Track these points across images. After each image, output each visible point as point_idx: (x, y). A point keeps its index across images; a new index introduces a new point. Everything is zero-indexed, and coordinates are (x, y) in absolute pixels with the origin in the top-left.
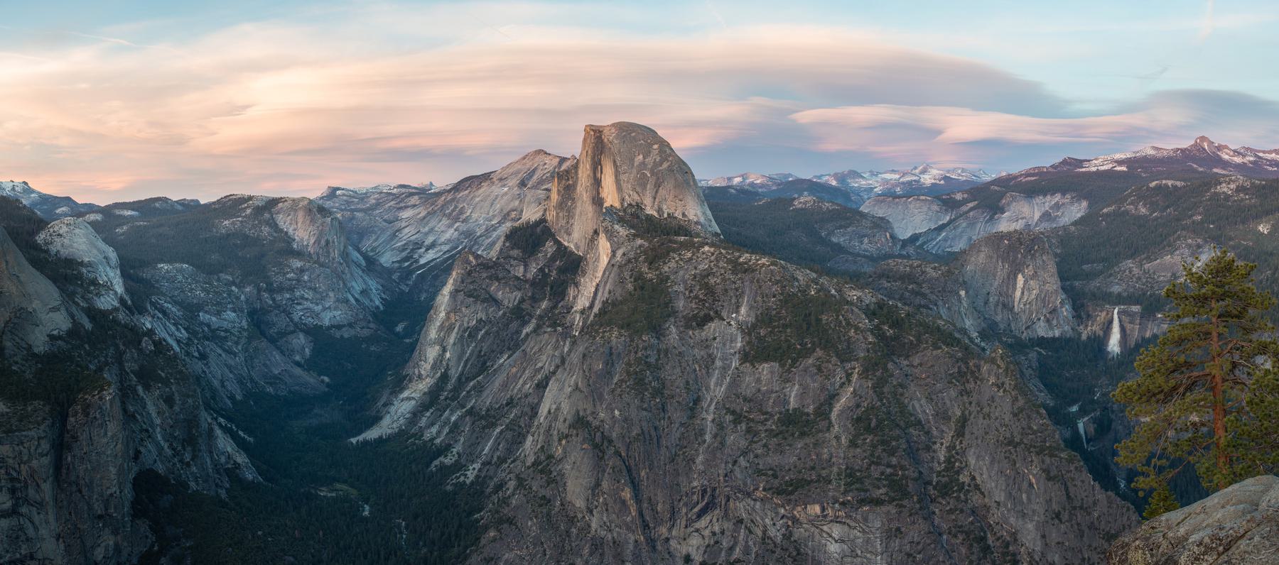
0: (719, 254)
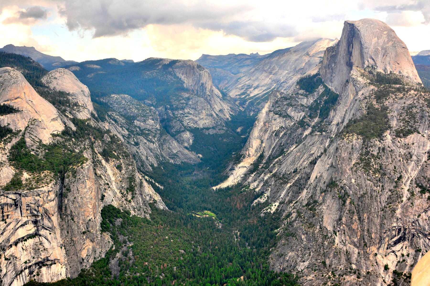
0: (420, 95)
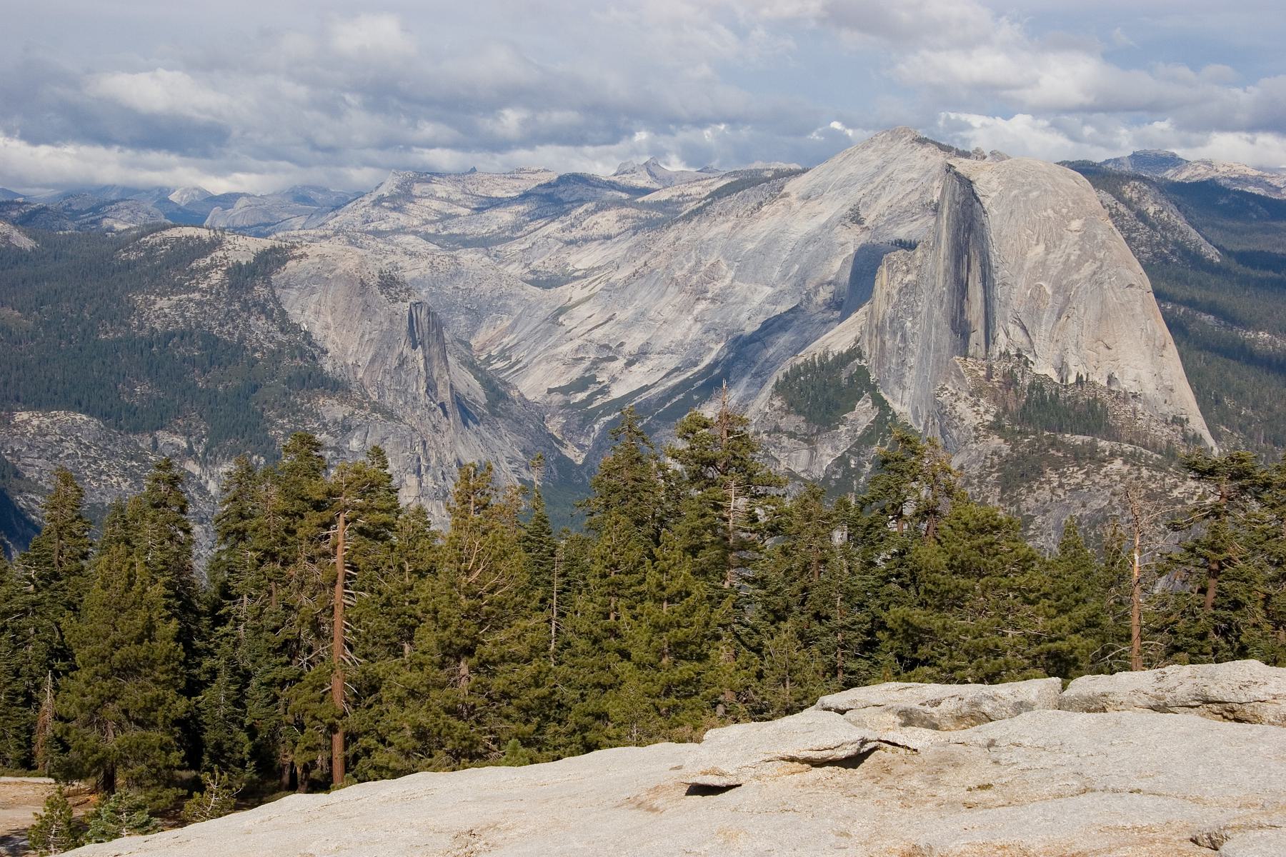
0: (1137, 478)
